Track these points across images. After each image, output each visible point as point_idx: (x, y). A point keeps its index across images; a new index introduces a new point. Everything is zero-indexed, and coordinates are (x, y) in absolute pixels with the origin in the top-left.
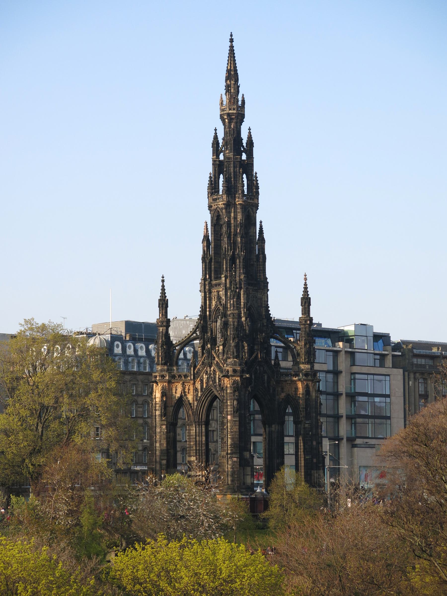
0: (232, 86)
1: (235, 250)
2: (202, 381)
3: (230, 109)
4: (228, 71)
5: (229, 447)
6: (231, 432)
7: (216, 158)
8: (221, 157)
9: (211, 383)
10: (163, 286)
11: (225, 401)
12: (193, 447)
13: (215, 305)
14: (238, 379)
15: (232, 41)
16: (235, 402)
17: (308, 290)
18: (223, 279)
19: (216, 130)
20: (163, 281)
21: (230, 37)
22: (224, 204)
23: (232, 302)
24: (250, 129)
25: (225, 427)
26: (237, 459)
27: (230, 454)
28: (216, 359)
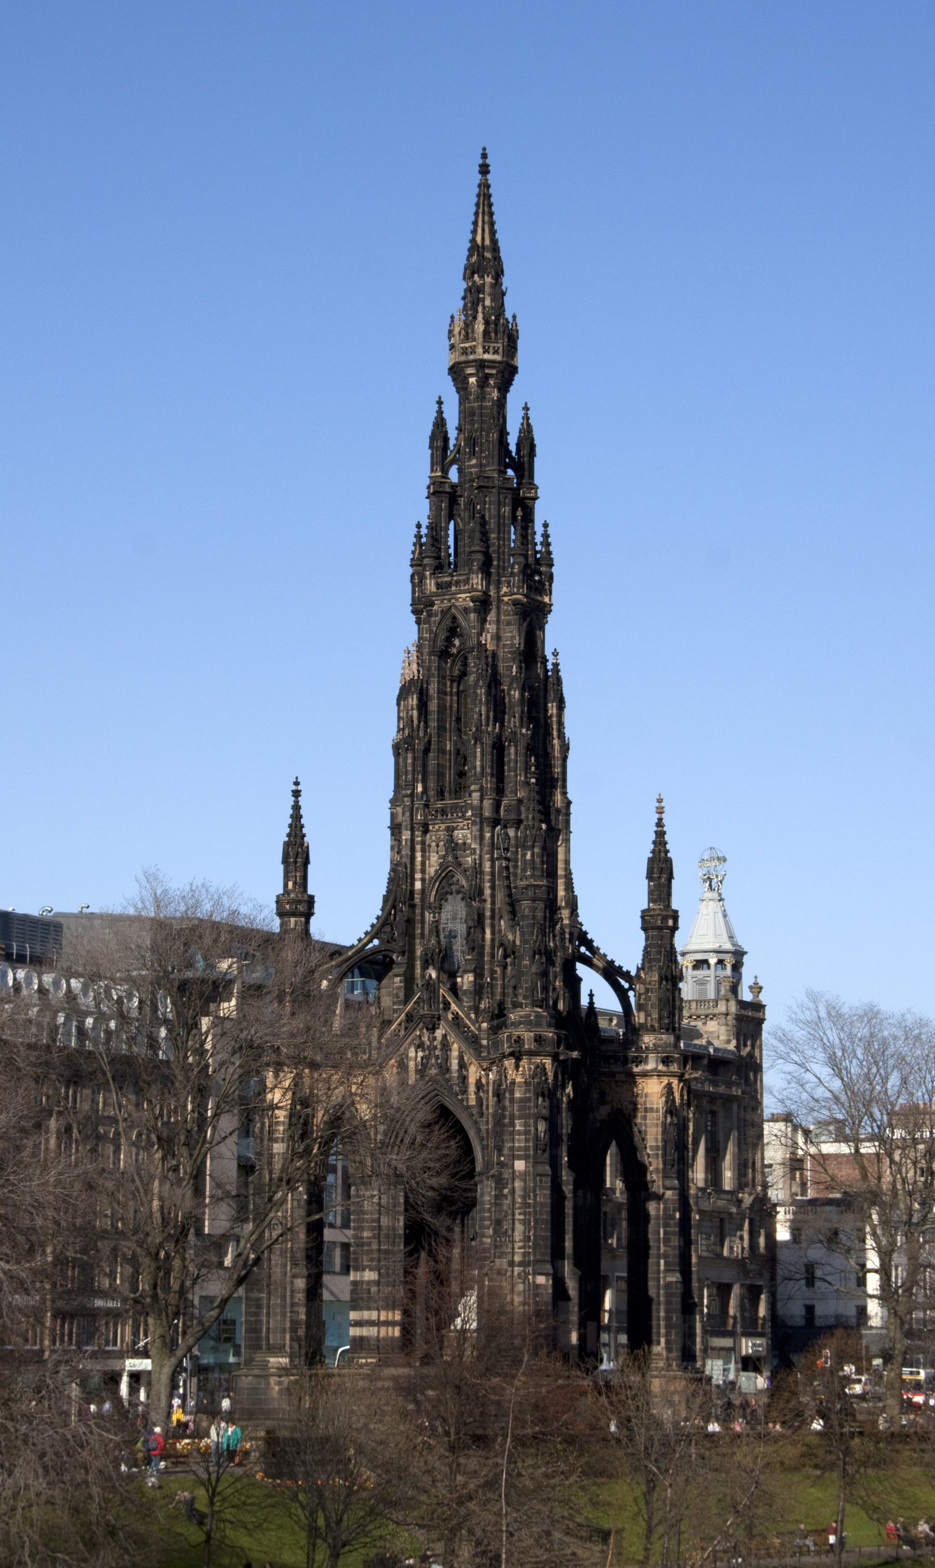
0: (487, 289)
1: (485, 721)
2: (402, 1066)
3: (486, 351)
4: (474, 248)
5: (517, 1245)
6: (525, 1205)
7: (443, 477)
8: (453, 475)
9: (433, 1071)
10: (296, 807)
11: (507, 1121)
12: (370, 1244)
13: (441, 865)
14: (548, 1062)
15: (484, 169)
16: (542, 1126)
17: (667, 837)
18: (476, 795)
19: (440, 403)
20: (296, 794)
21: (481, 161)
22: (473, 600)
23: (528, 857)
24: (526, 408)
25: (506, 1191)
26: (547, 1280)
27: (521, 1264)
28: (454, 1007)
